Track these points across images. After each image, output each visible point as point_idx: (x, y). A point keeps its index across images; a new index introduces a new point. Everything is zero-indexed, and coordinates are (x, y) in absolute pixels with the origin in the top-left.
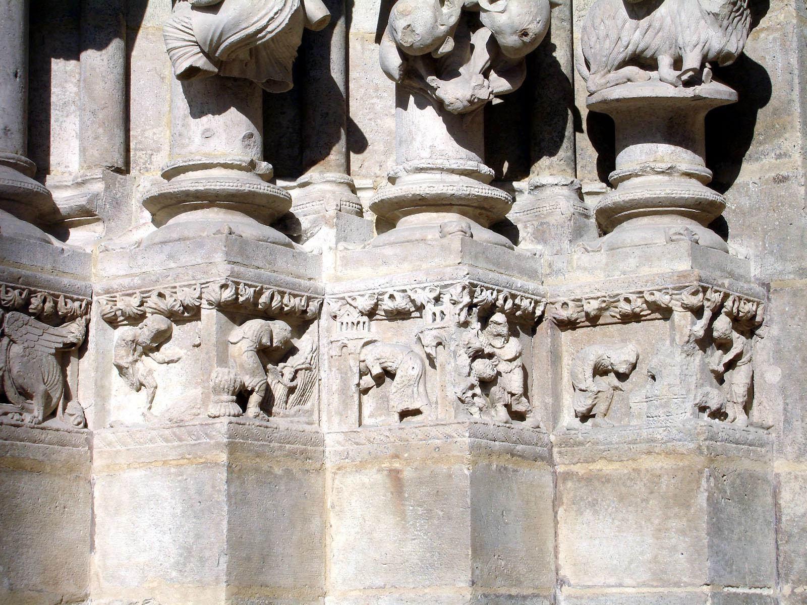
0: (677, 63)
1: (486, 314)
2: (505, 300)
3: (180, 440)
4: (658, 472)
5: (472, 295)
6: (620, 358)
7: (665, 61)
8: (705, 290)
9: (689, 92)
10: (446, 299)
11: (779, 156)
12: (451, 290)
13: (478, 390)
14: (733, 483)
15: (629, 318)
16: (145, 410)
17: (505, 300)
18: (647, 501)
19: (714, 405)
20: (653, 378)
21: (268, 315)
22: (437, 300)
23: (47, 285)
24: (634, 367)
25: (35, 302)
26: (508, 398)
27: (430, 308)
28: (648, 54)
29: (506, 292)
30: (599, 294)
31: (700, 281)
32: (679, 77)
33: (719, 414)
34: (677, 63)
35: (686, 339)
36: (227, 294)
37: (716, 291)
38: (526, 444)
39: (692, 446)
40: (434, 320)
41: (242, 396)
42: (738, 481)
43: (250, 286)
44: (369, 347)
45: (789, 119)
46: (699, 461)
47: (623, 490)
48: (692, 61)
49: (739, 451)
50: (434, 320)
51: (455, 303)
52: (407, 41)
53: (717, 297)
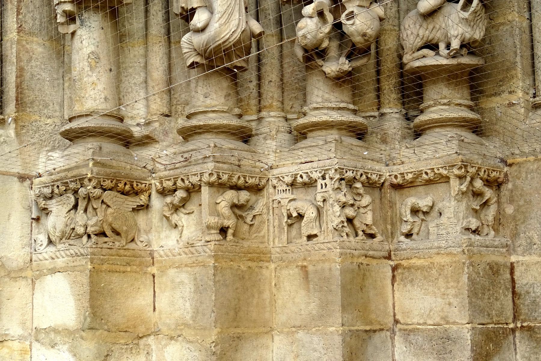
0: (448, 46)
1: (350, 183)
2: (361, 175)
3: (193, 254)
4: (443, 264)
5: (341, 173)
6: (424, 203)
7: (442, 46)
9: (454, 62)
11: (510, 93)
13: (346, 224)
14: (485, 268)
15: (429, 182)
17: (361, 175)
18: (437, 279)
19: (473, 227)
20: (441, 214)
21: (237, 188)
22: (324, 178)
23: (126, 176)
24: (432, 207)
25: (121, 185)
26: (365, 228)
27: (320, 182)
28: (434, 42)
29: (361, 171)
30: (412, 170)
31: (463, 162)
32: (449, 54)
33: (476, 232)
34: (448, 46)
36: (214, 178)
37: (472, 167)
38: (374, 250)
39: (460, 250)
40: (322, 188)
41: (223, 231)
42: (488, 267)
43: (226, 174)
45: (514, 72)
46: (463, 258)
47: (426, 274)
48: (455, 44)
49: (488, 251)
50: (322, 188)
51: (331, 179)
52: (304, 42)
53: (472, 170)
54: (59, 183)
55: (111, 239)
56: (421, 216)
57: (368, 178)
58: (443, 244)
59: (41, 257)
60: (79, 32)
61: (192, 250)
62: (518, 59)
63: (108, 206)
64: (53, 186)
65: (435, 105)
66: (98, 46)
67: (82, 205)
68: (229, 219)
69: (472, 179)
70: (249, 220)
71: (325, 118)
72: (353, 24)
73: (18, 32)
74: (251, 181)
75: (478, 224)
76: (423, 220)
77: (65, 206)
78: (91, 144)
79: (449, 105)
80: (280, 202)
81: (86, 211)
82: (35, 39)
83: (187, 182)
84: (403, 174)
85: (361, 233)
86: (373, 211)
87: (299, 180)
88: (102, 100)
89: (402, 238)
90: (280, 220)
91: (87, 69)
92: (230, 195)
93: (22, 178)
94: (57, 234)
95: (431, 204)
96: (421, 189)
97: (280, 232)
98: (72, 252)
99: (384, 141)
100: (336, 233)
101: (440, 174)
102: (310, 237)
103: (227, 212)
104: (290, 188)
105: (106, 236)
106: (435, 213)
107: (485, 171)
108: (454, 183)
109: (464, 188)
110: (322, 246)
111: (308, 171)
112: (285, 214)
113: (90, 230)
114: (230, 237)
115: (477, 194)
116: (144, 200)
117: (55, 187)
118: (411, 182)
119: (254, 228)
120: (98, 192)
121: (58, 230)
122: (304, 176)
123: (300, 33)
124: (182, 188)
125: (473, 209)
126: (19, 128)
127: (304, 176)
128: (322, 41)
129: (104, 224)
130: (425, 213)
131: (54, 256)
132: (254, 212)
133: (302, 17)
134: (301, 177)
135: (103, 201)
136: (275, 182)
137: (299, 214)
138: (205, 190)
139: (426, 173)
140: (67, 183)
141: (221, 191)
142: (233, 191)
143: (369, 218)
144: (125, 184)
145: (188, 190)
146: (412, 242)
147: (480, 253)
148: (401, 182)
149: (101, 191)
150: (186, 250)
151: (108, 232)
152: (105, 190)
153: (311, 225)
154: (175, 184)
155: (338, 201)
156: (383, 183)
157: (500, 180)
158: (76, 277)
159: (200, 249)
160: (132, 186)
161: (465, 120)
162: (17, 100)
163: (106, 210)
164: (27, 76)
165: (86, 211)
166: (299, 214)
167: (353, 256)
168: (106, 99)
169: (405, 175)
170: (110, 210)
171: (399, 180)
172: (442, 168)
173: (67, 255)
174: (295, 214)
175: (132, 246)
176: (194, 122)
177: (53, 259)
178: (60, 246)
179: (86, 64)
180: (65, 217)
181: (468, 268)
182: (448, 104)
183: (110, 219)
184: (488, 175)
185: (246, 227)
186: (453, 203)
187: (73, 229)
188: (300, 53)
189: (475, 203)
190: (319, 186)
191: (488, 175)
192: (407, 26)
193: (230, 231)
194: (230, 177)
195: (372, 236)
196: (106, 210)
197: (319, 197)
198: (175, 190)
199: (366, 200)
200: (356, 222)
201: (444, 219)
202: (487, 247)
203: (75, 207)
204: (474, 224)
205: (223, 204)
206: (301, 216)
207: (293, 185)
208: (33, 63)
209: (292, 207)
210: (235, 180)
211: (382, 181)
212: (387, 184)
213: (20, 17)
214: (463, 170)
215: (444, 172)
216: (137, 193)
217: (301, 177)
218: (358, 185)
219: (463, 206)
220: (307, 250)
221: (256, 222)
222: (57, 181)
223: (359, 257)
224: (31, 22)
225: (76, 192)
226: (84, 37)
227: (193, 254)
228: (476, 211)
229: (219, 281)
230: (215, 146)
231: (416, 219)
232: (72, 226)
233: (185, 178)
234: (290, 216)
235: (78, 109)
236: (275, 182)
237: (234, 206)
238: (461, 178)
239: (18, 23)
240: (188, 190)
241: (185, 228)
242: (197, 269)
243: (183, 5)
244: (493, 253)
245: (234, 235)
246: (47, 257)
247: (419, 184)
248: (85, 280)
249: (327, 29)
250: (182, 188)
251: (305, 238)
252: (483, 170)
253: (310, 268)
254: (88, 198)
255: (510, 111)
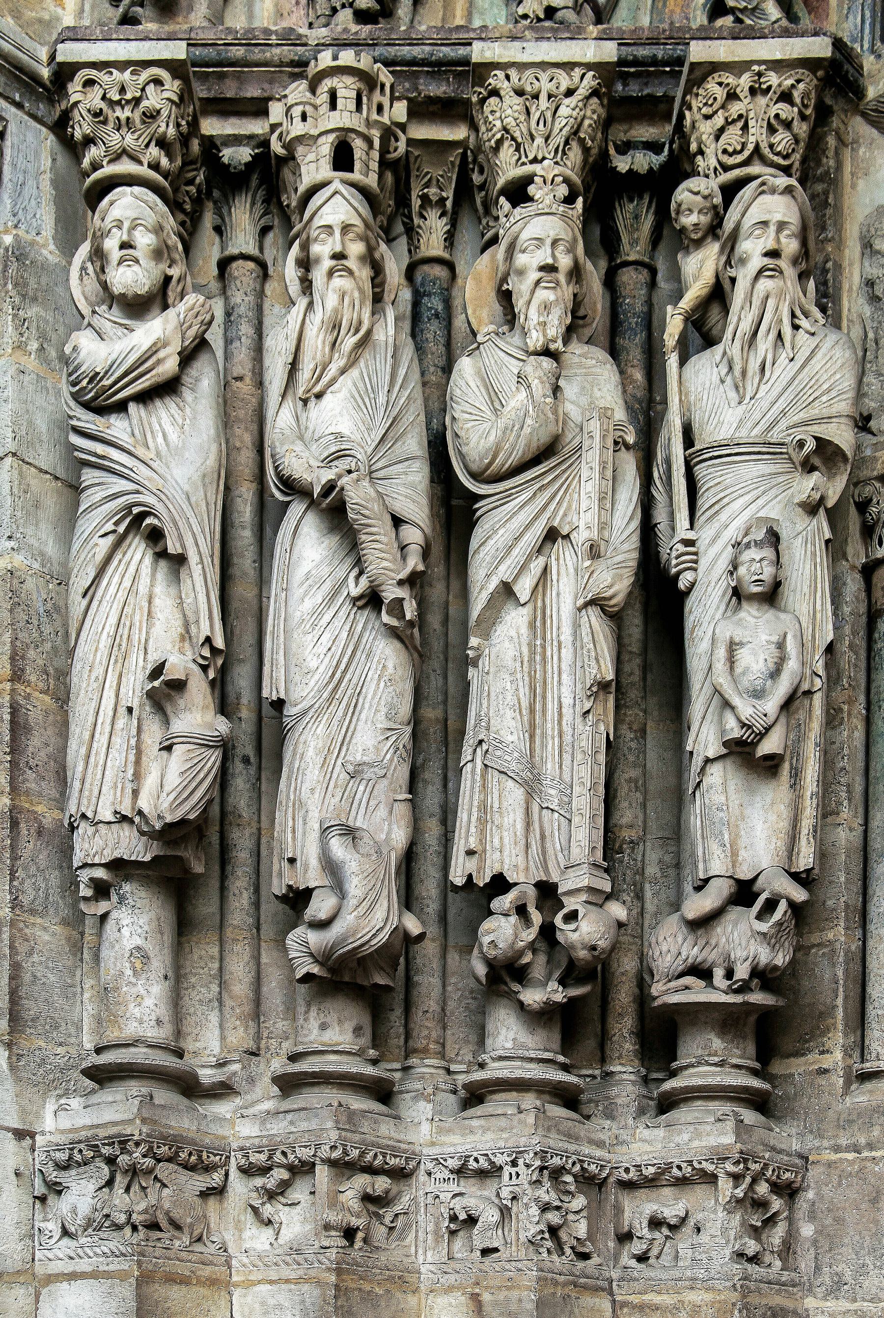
0: (729, 974)
1: (556, 1174)
2: (574, 1164)
3: (299, 1264)
4: (699, 1303)
6: (671, 1212)
7: (719, 973)
8: (746, 1161)
9: (738, 999)
10: (521, 1162)
12: (526, 1156)
16: (273, 1241)
17: (574, 1164)
19: (750, 1252)
20: (699, 1230)
22: (514, 1164)
23: (193, 1142)
24: (684, 1220)
25: (183, 1155)
27: (508, 1169)
30: (655, 1162)
32: (730, 986)
33: (754, 1259)
34: (729, 974)
35: (728, 1199)
36: (336, 1154)
37: (756, 1162)
40: (511, 1179)
41: (349, 1234)
43: (356, 1148)
44: (458, 1198)
48: (742, 972)
49: (771, 1289)
50: (511, 1179)
52: (492, 953)
53: (755, 1167)
54: (82, 1146)
55: (168, 1235)
56: (665, 1231)
57: (582, 1168)
58: (701, 1274)
59: (50, 1255)
60: (114, 915)
61: (299, 1258)
62: (840, 1001)
63: (164, 1185)
64: (72, 1149)
65: (699, 1064)
66: (146, 939)
67: (121, 1181)
68: (358, 1216)
69: (754, 1181)
70: (387, 1220)
71: (518, 1074)
72: (575, 931)
73: (13, 908)
74: (393, 1162)
75: (758, 1248)
76: (667, 1237)
77: (93, 1181)
78: (136, 1088)
79: (721, 1066)
80: (438, 1197)
81: (127, 1190)
82: (39, 920)
83: (291, 1157)
84: (640, 1166)
85: (568, 1251)
86: (588, 1218)
87: (472, 1164)
88: (153, 1023)
89: (633, 1263)
90: (437, 1224)
91: (129, 972)
92: (361, 1181)
93: (20, 1134)
94: (79, 1222)
95: (683, 1214)
96: (667, 1191)
97: (437, 1241)
98: (106, 1250)
99: (610, 1115)
100: (531, 1248)
101: (702, 1170)
102: (486, 1252)
103: (356, 1206)
104: (455, 1176)
105: (161, 1230)
106: (688, 1229)
107: (774, 1170)
108: (725, 1185)
109: (740, 1193)
110: (508, 1266)
111: (489, 1152)
112: (446, 1215)
113: (136, 1218)
114: (358, 1244)
115: (761, 1204)
116: (218, 1180)
117: (76, 1151)
118: (653, 1180)
119: (395, 1233)
120: (149, 1162)
121: (80, 1216)
122: (482, 1160)
123: (486, 940)
124: (281, 1166)
125: (752, 1226)
126: (14, 1058)
127: (482, 1160)
128: (521, 953)
129: (158, 1212)
130: (673, 1228)
131: (73, 1255)
132: (397, 1208)
133: (491, 913)
134: (476, 1160)
135: (156, 1177)
136: (430, 1165)
137: (469, 1216)
138: (322, 1173)
139: (679, 1168)
140: (97, 1146)
141: (347, 1173)
142: (367, 1176)
143: (581, 1229)
144: (190, 1154)
145: (291, 1168)
146: (650, 1269)
147: (759, 1291)
148: (635, 1178)
149: (153, 1161)
150: (288, 1258)
151: (164, 1223)
152: (159, 1161)
153: (489, 1234)
154: (270, 1158)
155: (537, 1200)
156: (606, 1179)
157: (797, 1185)
158: (112, 1287)
159: (311, 1257)
160: (200, 1157)
161: (746, 1089)
162: (10, 1015)
163: (160, 1191)
164: (27, 977)
165: (127, 1190)
166: (469, 1216)
167: (556, 1283)
168: (159, 1022)
169: (643, 1168)
170: (166, 1192)
171: (633, 1175)
172: (706, 1160)
173: (96, 1254)
174: (462, 1216)
175: (198, 1247)
176: (304, 1066)
177: (71, 1258)
178: (83, 1240)
179: (128, 965)
180: (94, 1197)
181: (740, 1312)
182: (721, 1064)
183: (167, 1205)
184: (778, 1177)
185: (383, 1230)
186: (721, 1214)
187: (107, 1216)
188: (481, 970)
189: (755, 1217)
190: (506, 1176)
191: (778, 1177)
192: (661, 939)
193: (360, 1235)
194: (363, 1154)
195: (585, 1256)
196: (160, 1191)
197: (505, 1193)
198: (270, 1169)
199: (579, 1202)
200: (563, 1235)
201: (704, 1238)
202: (770, 1283)
203: (110, 1183)
204: (752, 1247)
205: (350, 1194)
206: (472, 1221)
207: (460, 1172)
208: (36, 958)
209: (458, 1205)
210: (369, 1157)
211: (604, 1175)
212: (612, 1180)
213: (15, 883)
214: (741, 1166)
215: (710, 1167)
216: (208, 1169)
217: (476, 1160)
218: (568, 1178)
219: (737, 1219)
220: (481, 1270)
221: (399, 1223)
222: (80, 1142)
223: (565, 1285)
224: (31, 893)
225: (111, 1161)
226: (125, 922)
227: (299, 1264)
228: (755, 1229)
229: (342, 1306)
230: (340, 1105)
231: (657, 1235)
232: (105, 1211)
233: (289, 1151)
234: (454, 1218)
235: (113, 1035)
236: (430, 1165)
237: (367, 1198)
238: (737, 1178)
239: (11, 893)
240: (291, 1168)
241: (284, 1226)
242: (306, 1287)
243: (291, 883)
244: (779, 1292)
245: (365, 1240)
246: (61, 1256)
247: (664, 1183)
248: (127, 1291)
249: (530, 934)
250: (281, 1166)
251: (479, 1253)
252: (771, 1169)
253: (486, 1297)
254: (133, 1172)
255: (822, 1081)
